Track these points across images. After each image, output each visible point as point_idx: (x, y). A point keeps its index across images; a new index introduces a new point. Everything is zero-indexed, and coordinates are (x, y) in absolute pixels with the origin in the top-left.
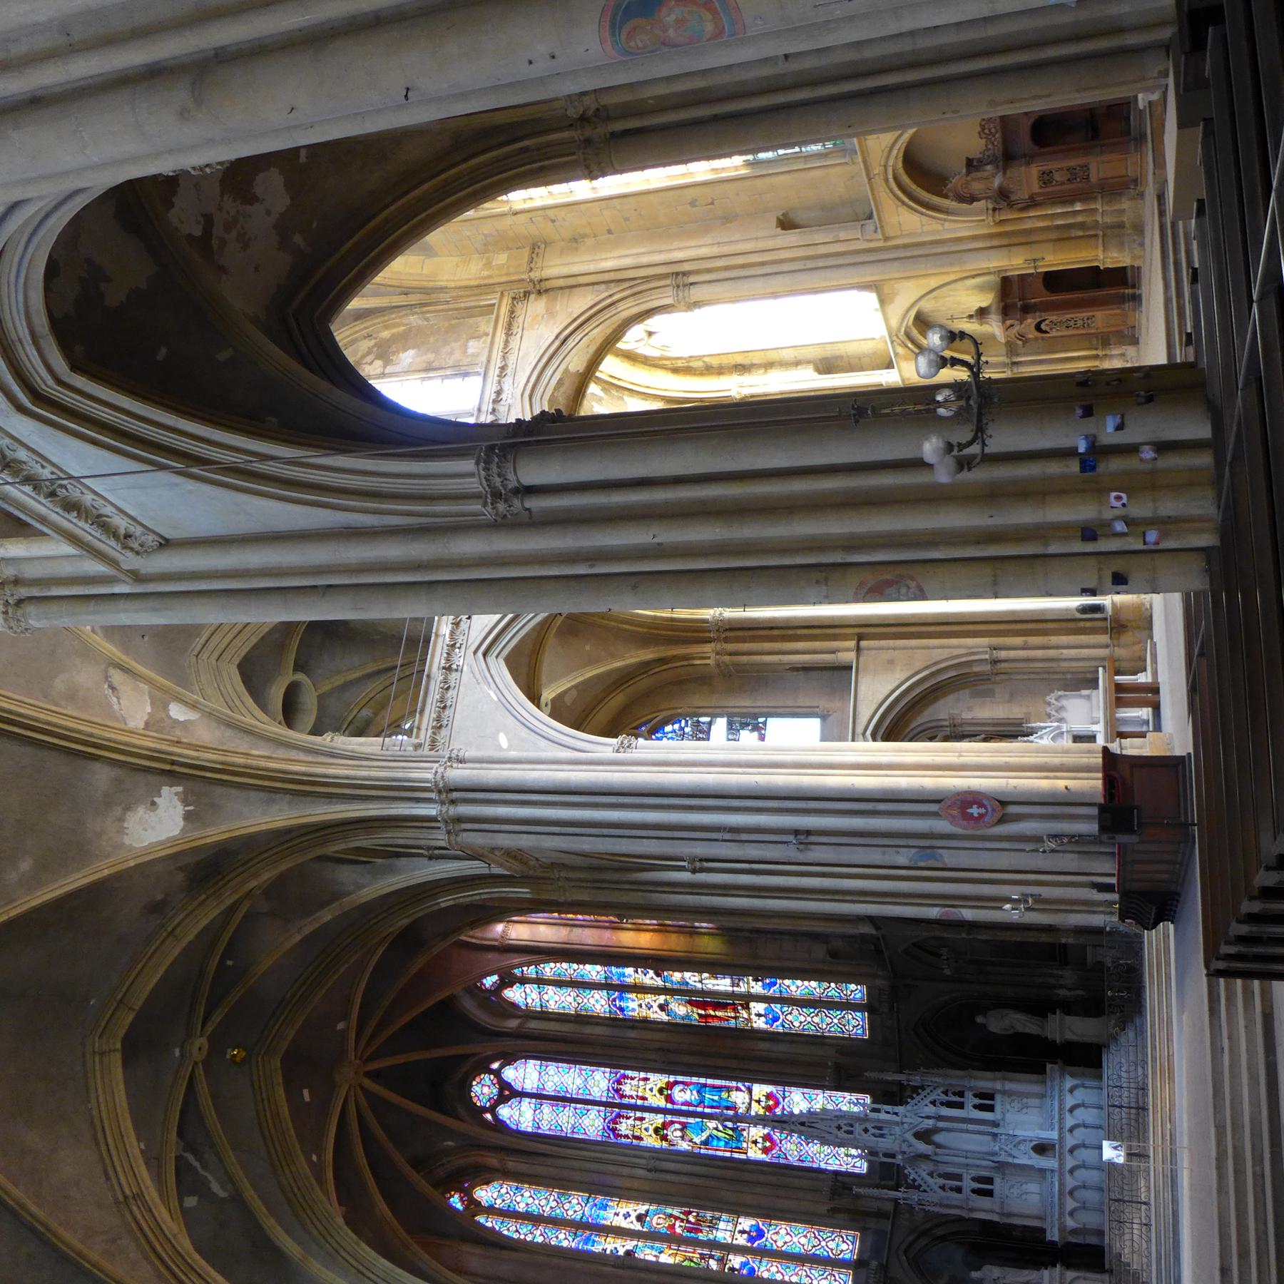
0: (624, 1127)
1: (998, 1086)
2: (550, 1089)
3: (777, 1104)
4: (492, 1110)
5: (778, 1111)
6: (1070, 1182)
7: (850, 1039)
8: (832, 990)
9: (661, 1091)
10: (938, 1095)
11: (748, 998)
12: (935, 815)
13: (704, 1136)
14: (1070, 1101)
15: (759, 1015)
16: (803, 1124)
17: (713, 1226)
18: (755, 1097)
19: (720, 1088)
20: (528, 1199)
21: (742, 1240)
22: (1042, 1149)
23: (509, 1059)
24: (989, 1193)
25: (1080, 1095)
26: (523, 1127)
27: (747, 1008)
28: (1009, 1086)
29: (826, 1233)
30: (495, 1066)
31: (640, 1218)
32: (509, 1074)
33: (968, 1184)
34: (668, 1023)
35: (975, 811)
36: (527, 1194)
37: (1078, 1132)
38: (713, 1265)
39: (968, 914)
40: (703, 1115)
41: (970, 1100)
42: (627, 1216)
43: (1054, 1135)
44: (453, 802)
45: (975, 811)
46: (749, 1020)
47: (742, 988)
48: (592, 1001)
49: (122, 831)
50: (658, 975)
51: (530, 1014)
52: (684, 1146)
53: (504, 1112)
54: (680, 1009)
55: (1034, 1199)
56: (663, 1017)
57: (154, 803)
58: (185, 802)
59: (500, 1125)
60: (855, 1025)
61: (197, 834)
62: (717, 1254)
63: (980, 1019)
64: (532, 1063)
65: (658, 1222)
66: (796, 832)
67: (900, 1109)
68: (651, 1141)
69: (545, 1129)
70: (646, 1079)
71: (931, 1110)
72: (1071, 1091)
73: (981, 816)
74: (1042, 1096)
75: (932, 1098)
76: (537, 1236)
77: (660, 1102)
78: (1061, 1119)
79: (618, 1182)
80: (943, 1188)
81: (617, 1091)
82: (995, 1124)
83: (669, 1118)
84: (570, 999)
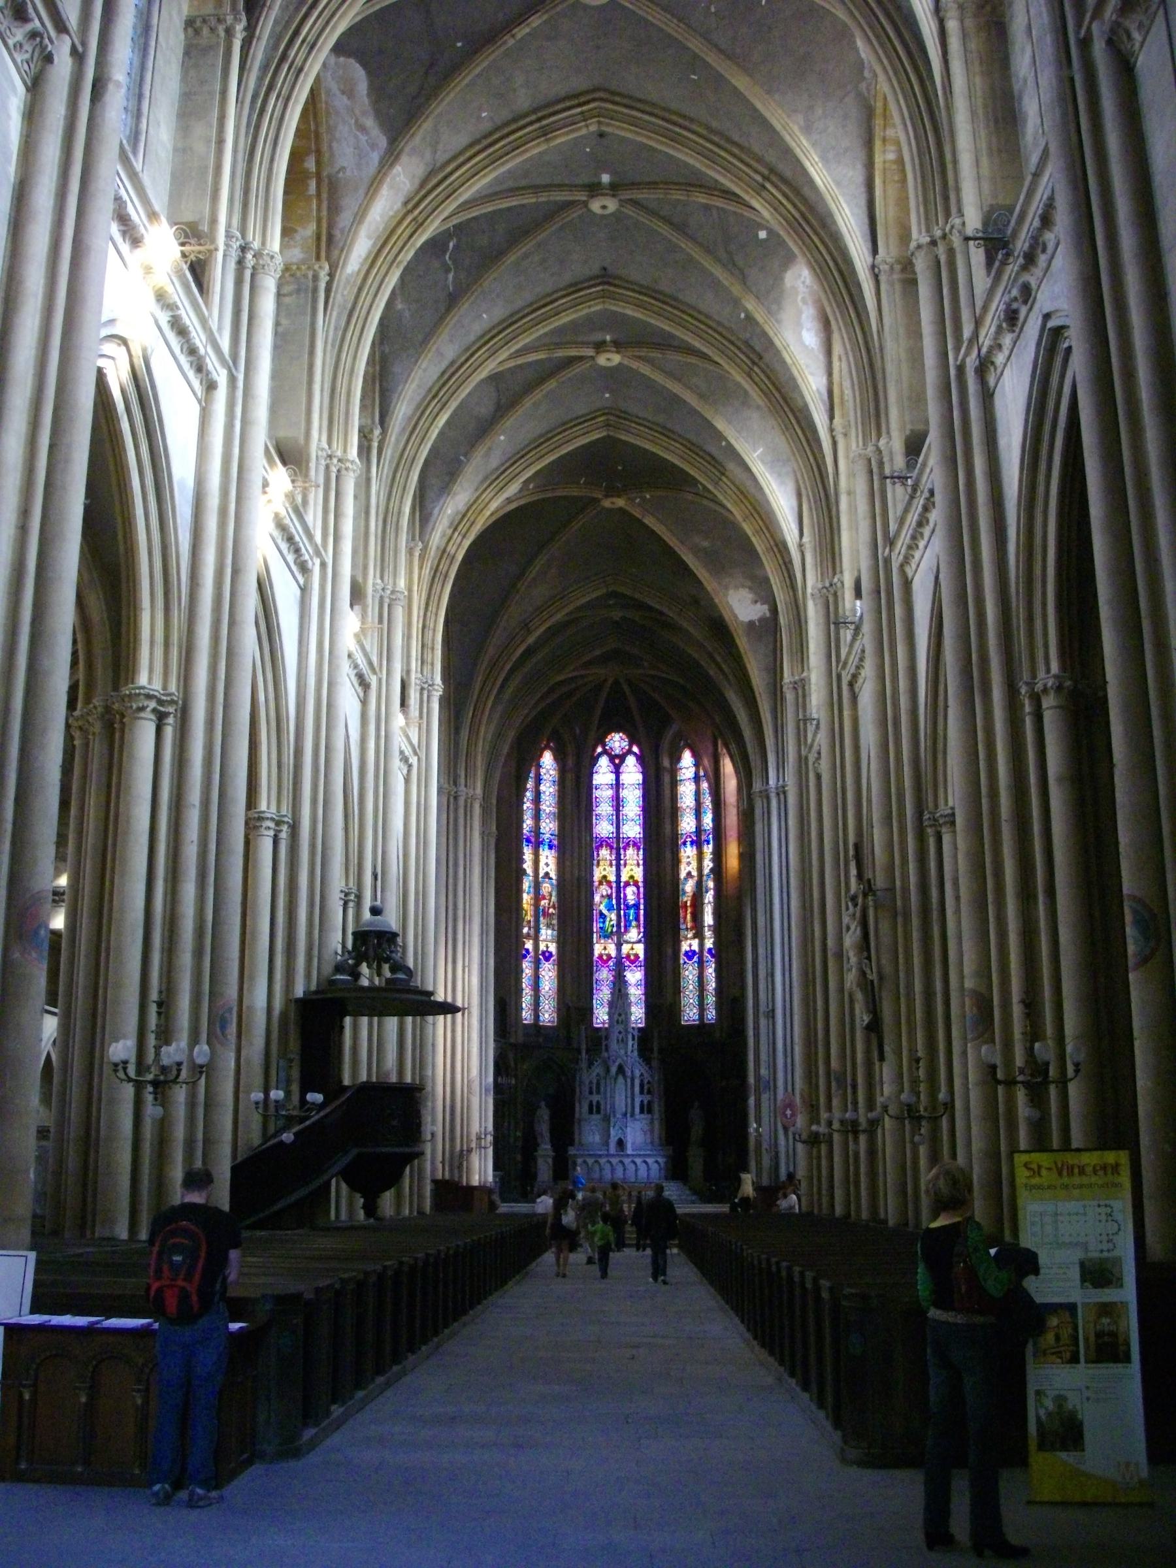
0: (604, 853)
1: (656, 1116)
2: (624, 793)
3: (632, 962)
4: (605, 752)
5: (627, 963)
6: (603, 1161)
7: (680, 1011)
8: (711, 1000)
9: (632, 877)
10: (647, 1077)
11: (699, 935)
12: (786, 1089)
13: (605, 912)
14: (650, 1161)
15: (690, 946)
16: (620, 990)
17: (548, 926)
18: (635, 946)
19: (637, 919)
20: (548, 790)
21: (542, 947)
22: (621, 1144)
23: (640, 759)
24: (591, 1112)
25: (655, 1167)
26: (595, 776)
27: (694, 937)
28: (657, 1124)
29: (553, 1003)
30: (635, 749)
31: (547, 874)
32: (631, 761)
33: (595, 1098)
34: (678, 879)
35: (789, 1112)
36: (551, 790)
37: (633, 1166)
38: (525, 930)
39: (752, 1101)
40: (619, 909)
41: (647, 1098)
42: (547, 865)
43: (629, 1152)
44: (778, 794)
45: (789, 1112)
46: (686, 939)
47: (708, 933)
48: (688, 820)
49: (736, 587)
50: (712, 870)
51: (674, 772)
52: (597, 898)
53: (604, 761)
54: (689, 887)
55: (590, 1139)
56: (683, 875)
57: (756, 602)
58: (761, 620)
59: (595, 760)
60: (690, 1014)
61: (740, 632)
62: (532, 932)
63: (696, 1104)
64: (640, 777)
65: (546, 888)
66: (773, 1010)
67: (636, 1053)
68: (598, 874)
69: (596, 793)
70: (638, 865)
71: (637, 1073)
72: (657, 1162)
73: (786, 1116)
74: (652, 1143)
75: (646, 1075)
76: (527, 805)
77: (624, 878)
78: (640, 1156)
79: (567, 856)
80: (591, 1083)
81: (628, 844)
82: (633, 1115)
83: (614, 885)
84: (688, 803)
